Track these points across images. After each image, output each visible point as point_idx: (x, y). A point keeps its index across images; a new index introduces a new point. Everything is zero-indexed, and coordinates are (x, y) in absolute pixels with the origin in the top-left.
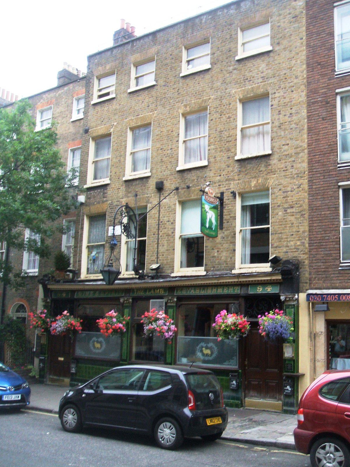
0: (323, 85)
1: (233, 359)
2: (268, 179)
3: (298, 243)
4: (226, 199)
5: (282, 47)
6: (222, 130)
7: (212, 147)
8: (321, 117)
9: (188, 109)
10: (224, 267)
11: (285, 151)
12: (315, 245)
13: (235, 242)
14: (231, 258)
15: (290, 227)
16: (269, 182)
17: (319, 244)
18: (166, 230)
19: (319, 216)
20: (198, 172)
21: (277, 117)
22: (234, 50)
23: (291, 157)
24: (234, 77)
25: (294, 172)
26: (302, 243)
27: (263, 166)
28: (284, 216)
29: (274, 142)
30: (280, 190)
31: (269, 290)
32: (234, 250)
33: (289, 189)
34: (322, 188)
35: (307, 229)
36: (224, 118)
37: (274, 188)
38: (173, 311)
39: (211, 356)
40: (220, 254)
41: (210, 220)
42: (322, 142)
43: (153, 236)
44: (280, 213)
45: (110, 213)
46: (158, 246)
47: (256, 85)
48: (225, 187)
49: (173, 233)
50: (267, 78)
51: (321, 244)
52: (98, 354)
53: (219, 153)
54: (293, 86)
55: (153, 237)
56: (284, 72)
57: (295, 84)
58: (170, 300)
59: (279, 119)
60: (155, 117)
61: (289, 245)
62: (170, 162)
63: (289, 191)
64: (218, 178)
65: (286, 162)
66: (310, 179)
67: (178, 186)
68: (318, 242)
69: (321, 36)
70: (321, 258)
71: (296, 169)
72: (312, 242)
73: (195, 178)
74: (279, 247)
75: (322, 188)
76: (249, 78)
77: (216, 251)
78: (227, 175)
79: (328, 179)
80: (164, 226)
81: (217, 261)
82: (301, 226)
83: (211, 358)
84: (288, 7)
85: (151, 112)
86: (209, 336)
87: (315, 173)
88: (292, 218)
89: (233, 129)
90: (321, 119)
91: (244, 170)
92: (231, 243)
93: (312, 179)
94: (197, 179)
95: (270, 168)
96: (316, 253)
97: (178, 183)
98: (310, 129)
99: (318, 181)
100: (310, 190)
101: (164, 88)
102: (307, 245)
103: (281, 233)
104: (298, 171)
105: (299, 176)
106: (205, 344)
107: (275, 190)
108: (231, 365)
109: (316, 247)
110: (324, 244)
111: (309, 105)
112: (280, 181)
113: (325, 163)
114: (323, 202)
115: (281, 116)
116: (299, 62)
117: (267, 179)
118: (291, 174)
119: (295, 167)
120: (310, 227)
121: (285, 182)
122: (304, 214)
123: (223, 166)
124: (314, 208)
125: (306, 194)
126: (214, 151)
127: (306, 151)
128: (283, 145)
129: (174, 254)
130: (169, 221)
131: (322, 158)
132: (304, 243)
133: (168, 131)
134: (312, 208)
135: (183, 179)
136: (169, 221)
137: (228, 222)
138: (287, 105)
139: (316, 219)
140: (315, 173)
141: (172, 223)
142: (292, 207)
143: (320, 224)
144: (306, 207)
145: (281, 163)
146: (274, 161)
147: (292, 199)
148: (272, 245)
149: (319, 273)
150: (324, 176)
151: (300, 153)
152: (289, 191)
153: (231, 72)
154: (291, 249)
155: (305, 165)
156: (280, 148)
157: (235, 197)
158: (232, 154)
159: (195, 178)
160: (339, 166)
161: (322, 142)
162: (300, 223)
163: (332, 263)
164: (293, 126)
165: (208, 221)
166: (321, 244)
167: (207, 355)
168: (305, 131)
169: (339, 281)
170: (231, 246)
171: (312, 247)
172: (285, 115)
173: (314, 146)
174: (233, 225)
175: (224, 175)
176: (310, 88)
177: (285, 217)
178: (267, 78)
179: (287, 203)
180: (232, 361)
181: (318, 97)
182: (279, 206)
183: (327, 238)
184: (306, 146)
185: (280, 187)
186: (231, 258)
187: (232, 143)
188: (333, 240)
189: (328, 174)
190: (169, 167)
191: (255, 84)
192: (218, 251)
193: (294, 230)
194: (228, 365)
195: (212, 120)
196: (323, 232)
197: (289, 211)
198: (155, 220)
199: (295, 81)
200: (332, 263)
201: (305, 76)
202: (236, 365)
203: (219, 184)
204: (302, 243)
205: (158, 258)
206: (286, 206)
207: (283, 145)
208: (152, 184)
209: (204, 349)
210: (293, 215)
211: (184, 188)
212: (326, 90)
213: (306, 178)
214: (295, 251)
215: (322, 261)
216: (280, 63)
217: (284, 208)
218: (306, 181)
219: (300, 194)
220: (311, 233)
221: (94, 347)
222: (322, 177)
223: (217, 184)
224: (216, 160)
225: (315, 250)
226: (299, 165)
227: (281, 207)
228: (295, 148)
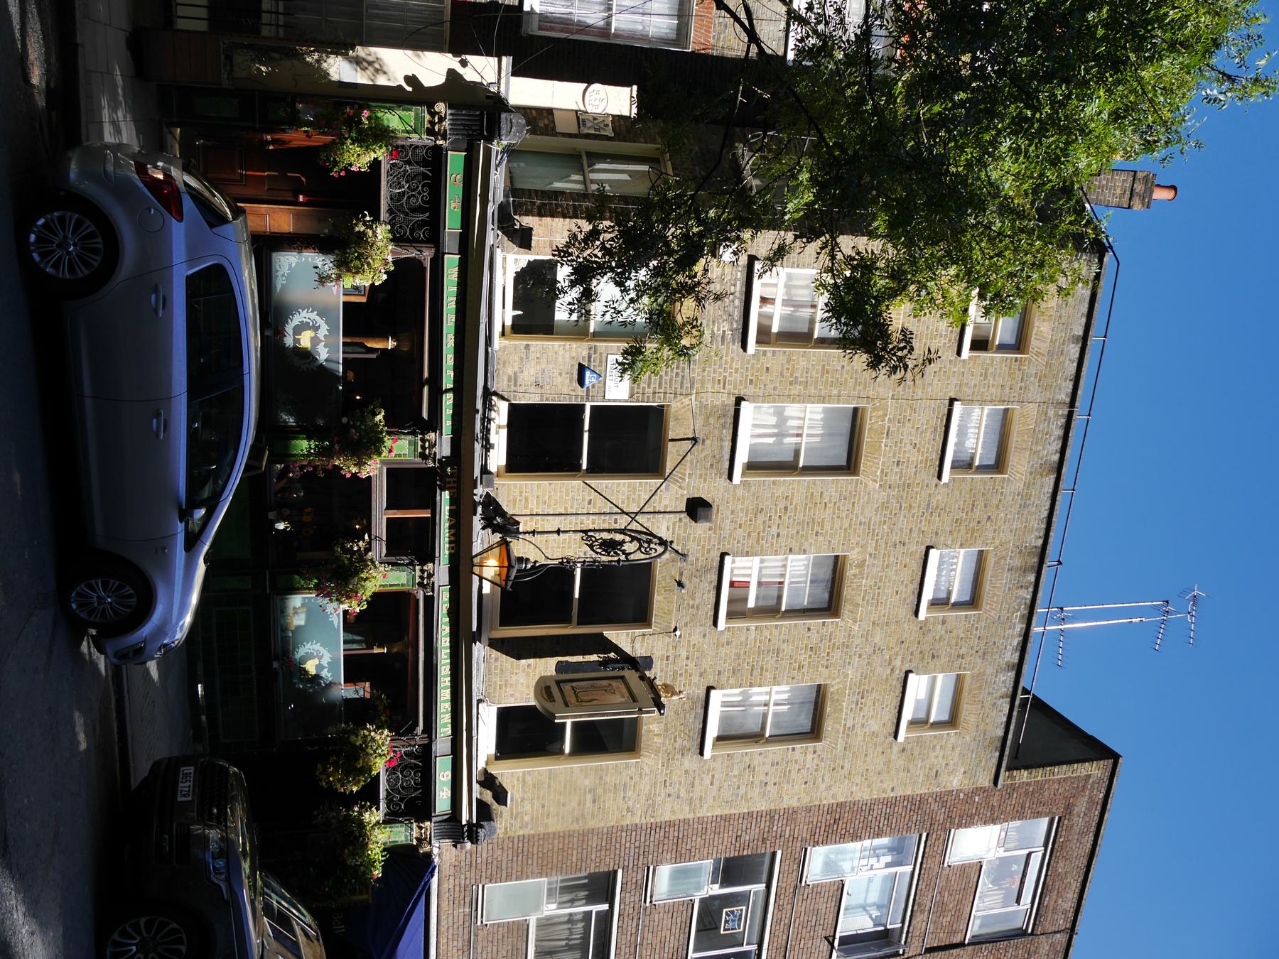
0: (796, 832)
2: (656, 755)
3: (526, 818)
5: (893, 757)
6: (781, 655)
8: (744, 833)
9: (850, 572)
10: (495, 682)
11: (702, 779)
12: (520, 845)
15: (559, 801)
16: (650, 757)
17: (520, 851)
19: (571, 846)
20: (709, 606)
21: (769, 761)
22: (932, 665)
23: (688, 792)
24: (879, 670)
25: (658, 799)
26: (527, 824)
27: (685, 743)
28: (580, 790)
29: (723, 759)
30: (631, 778)
31: (442, 794)
33: (629, 793)
34: (618, 846)
35: (551, 830)
36: (803, 657)
37: (636, 768)
38: (403, 585)
42: (699, 839)
43: (587, 498)
44: (587, 782)
47: (844, 716)
50: (848, 735)
51: (521, 855)
53: (734, 651)
54: (814, 784)
56: (847, 766)
57: (818, 787)
59: (764, 764)
60: (866, 486)
61: (526, 803)
62: (749, 535)
63: (625, 793)
64: (684, 655)
65: (680, 783)
66: (639, 826)
67: (691, 558)
68: (525, 849)
69: (882, 819)
70: (495, 856)
71: (664, 802)
72: (526, 840)
73: (697, 601)
74: (523, 786)
75: (618, 846)
76: (864, 701)
78: (686, 672)
79: (632, 854)
82: (558, 820)
84: (960, 763)
85: (882, 472)
87: (648, 832)
88: (574, 804)
89: (775, 678)
90: (739, 833)
93: (639, 830)
94: (693, 607)
95: (678, 756)
96: (506, 848)
97: (697, 559)
98: (726, 819)
99: (633, 838)
100: (620, 828)
101: (923, 505)
102: (521, 833)
103: (550, 786)
104: (659, 805)
105: (651, 808)
107: (633, 769)
109: (516, 847)
110: (520, 858)
111: (771, 816)
112: (647, 778)
113: (661, 846)
114: (594, 850)
115: (767, 768)
116: (854, 789)
117: (657, 752)
118: (655, 794)
119: (668, 799)
120: (554, 833)
121: (645, 786)
122: (577, 823)
123: (704, 665)
124: (586, 838)
125: (612, 824)
126: (743, 639)
127: (691, 816)
128: (713, 776)
131: (671, 842)
132: (526, 827)
133: (821, 524)
134: (585, 835)
135: (701, 571)
138: (785, 775)
139: (566, 841)
140: (648, 832)
142: (594, 801)
143: (556, 850)
144: (592, 824)
145: (680, 776)
146: (690, 762)
147: (609, 800)
148: (529, 772)
149: (468, 856)
150: (639, 847)
151: (690, 806)
152: (625, 793)
153: (890, 664)
154: (517, 806)
155: (667, 816)
156: (709, 771)
158: (726, 679)
159: (697, 601)
160: (651, 868)
161: (699, 839)
162: (563, 818)
163: (484, 874)
164: (742, 791)
166: (521, 855)
168: (727, 811)
169: (451, 886)
171: (516, 841)
172: (767, 774)
173: (695, 826)
175: (687, 665)
176: (799, 812)
177: (578, 791)
178: (848, 735)
179: (605, 791)
181: (780, 825)
182: (601, 778)
183: (530, 862)
184: (701, 815)
185: (637, 778)
187: (747, 678)
188: (525, 872)
189: (641, 853)
190: (740, 533)
191: (846, 714)
193: (551, 809)
195: (809, 629)
196: (540, 855)
197: (589, 797)
199: (822, 787)
200: (484, 874)
201: (825, 802)
204: (527, 824)
206: (599, 791)
207: (713, 776)
209: (316, 661)
210: (579, 804)
211: (681, 574)
212: (787, 836)
213: (643, 818)
214: (512, 814)
215: (490, 859)
216: (866, 755)
217: (595, 789)
218: (637, 821)
219: (616, 812)
220: (542, 837)
222: (637, 844)
223: (671, 653)
224: (723, 646)
225: (511, 846)
226: (668, 805)
227: (597, 782)
228: (701, 797)
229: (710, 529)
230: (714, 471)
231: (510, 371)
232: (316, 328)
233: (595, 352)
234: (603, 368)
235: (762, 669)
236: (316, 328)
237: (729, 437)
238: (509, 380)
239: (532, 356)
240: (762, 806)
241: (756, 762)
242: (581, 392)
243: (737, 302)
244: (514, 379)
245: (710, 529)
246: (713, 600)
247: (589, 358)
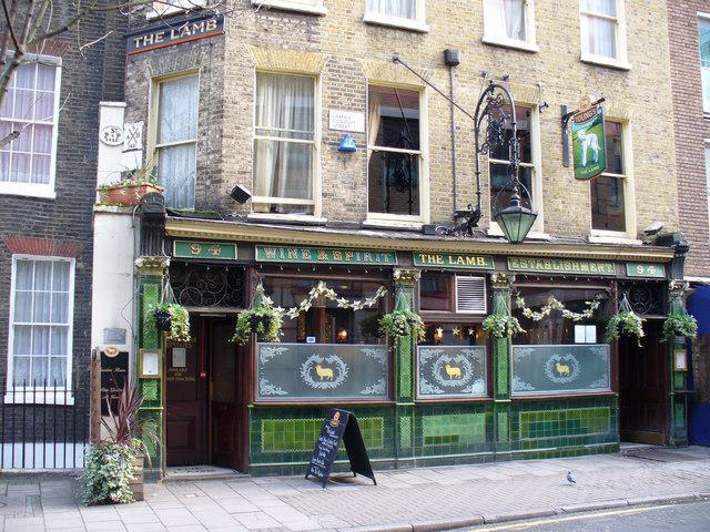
7: (542, 24)
39: (462, 377)
45: (330, 79)
46: (454, 172)
52: (329, 392)
53: (553, 39)
55: (442, 153)
64: (556, 80)
83: (569, 380)
91: (594, 80)
98: (673, 56)
105: (663, 113)
121: (648, 117)
134: (681, 165)
144: (673, 160)
146: (633, 79)
168: (668, 53)
180: (601, 381)
184: (670, 74)
190: (466, 29)
192: (563, 202)
205: (454, 196)
209: (558, 365)
221: (316, 377)
229: (463, 52)
230: (419, 46)
231: (343, 210)
232: (315, 364)
233: (327, 139)
234: (340, 133)
235: (566, 18)
236: (315, 364)
237: (392, 32)
238: (351, 210)
239: (331, 191)
240: (665, 25)
241: (635, 28)
242: (359, 152)
243: (286, 20)
244: (350, 206)
245: (463, 52)
246: (517, 54)
247: (331, 144)
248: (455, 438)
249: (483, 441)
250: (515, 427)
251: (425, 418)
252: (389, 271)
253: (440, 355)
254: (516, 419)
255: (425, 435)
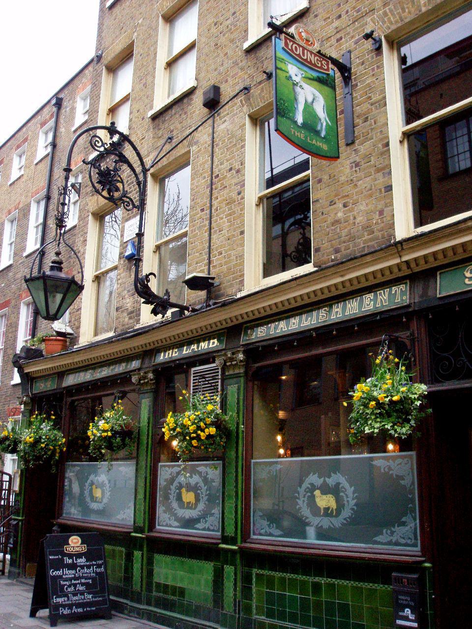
1: (404, 524)
4: (358, 65)
13: (389, 166)
14: (381, 213)
18: (226, 191)
32: (389, 188)
38: (239, 389)
40: (352, 210)
41: (309, 107)
46: (210, 235)
48: (352, 37)
49: (239, 194)
58: (231, 359)
64: (336, 23)
67: (247, 83)
77: (341, 206)
80: (222, 184)
81: (344, 233)
86: (340, 454)
92: (378, 170)
106: (320, 477)
108: (397, 544)
129: (242, 245)
130: (231, 169)
136: (231, 169)
137: (366, 120)
141: (238, 171)
157: (379, 50)
165: (301, 107)
167: (327, 512)
170: (381, 180)
174: (381, 121)
175: (347, 12)
180: (400, 531)
186: (381, 213)
192: (345, 206)
194: (389, 543)
198: (205, 178)
202: (415, 545)
203: (338, 36)
208: (198, 100)
209: (317, 493)
248: (182, 592)
249: (210, 605)
250: (246, 591)
251: (157, 557)
252: (126, 377)
253: (178, 473)
254: (247, 579)
255: (156, 579)
